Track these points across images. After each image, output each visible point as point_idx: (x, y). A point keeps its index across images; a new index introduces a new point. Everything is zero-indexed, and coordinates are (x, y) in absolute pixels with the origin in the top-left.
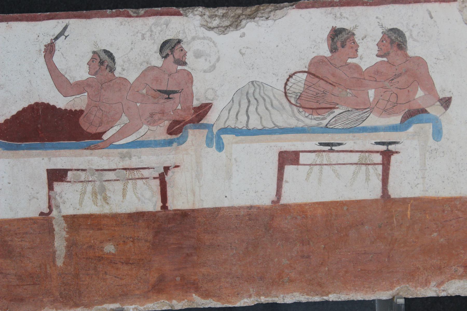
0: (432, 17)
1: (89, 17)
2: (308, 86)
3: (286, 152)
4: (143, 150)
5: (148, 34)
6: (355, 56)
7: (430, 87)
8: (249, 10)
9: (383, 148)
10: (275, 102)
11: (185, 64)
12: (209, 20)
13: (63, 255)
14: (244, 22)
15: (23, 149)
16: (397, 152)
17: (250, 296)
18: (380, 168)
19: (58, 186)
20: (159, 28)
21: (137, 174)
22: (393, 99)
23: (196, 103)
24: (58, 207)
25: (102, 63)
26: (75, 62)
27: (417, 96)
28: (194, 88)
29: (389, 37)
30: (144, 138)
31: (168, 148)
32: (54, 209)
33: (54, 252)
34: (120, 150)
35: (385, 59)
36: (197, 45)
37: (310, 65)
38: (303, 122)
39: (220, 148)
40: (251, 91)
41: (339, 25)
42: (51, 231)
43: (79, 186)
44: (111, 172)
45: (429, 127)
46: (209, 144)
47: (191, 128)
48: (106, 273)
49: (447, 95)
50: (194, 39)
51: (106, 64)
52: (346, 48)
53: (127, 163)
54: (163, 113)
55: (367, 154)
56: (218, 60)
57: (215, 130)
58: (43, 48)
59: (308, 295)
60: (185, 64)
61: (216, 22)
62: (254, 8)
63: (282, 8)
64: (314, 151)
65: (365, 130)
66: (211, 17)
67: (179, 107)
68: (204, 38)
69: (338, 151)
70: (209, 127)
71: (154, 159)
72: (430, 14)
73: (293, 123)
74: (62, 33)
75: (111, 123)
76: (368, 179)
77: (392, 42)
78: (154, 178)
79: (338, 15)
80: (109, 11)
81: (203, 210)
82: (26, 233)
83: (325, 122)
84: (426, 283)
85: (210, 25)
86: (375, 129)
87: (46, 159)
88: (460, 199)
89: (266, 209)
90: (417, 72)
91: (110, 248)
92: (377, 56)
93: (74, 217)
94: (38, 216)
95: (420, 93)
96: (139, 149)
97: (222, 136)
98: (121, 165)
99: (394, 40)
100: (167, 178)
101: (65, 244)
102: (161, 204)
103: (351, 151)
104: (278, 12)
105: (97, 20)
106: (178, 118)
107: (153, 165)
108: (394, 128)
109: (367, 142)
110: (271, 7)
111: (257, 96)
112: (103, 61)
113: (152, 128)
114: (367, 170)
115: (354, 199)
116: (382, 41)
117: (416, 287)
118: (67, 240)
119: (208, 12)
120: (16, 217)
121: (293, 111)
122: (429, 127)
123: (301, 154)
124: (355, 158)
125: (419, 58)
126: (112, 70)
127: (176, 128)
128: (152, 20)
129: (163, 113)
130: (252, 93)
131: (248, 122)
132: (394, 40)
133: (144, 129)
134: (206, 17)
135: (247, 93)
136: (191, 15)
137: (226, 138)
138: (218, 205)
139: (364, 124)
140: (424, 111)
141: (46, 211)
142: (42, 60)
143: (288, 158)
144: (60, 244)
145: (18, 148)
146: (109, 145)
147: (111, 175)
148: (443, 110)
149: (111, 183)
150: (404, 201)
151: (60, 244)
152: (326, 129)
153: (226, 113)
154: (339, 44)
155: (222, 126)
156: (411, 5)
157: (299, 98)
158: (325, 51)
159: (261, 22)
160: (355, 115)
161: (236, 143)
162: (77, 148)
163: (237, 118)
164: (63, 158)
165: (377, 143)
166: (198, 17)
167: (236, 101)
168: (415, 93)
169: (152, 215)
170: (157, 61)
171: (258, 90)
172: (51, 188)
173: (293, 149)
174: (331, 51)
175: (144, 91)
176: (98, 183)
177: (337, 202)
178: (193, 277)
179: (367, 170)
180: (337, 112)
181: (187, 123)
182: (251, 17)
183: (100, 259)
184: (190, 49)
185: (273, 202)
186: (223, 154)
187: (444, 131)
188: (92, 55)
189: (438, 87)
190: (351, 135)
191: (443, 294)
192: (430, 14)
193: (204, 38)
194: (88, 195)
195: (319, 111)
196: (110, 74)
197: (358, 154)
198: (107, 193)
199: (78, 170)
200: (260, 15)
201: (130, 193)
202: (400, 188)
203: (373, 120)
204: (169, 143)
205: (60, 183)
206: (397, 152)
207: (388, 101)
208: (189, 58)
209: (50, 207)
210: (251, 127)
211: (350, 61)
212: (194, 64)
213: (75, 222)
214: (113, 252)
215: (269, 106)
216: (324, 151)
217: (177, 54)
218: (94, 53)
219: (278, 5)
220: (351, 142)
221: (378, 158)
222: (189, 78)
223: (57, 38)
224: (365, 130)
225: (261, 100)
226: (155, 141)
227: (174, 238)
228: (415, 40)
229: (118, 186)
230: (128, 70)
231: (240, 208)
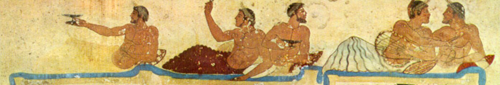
6: (427, 22)
7: (480, 49)
10: (367, 52)
11: (305, 22)
22: (452, 56)
40: (351, 44)
46: (319, 79)
49: (492, 54)
57: (324, 71)
58: (204, 5)
60: (305, 22)
75: (252, 61)
83: (402, 69)
90: (471, 36)
97: (329, 76)
99: (455, 12)
111: (355, 48)
112: (246, 15)
130: (351, 44)
132: (455, 12)
139: (432, 71)
142: (203, 14)
146: (248, 78)
148: (487, 64)
152: (403, 74)
153: (332, 58)
155: (329, 69)
157: (385, 50)
158: (405, 17)
167: (340, 51)
170: (285, 18)
180: (412, 62)
189: (485, 47)
210: (349, 70)
211: (423, 25)
212: (310, 23)
230: (264, 23)
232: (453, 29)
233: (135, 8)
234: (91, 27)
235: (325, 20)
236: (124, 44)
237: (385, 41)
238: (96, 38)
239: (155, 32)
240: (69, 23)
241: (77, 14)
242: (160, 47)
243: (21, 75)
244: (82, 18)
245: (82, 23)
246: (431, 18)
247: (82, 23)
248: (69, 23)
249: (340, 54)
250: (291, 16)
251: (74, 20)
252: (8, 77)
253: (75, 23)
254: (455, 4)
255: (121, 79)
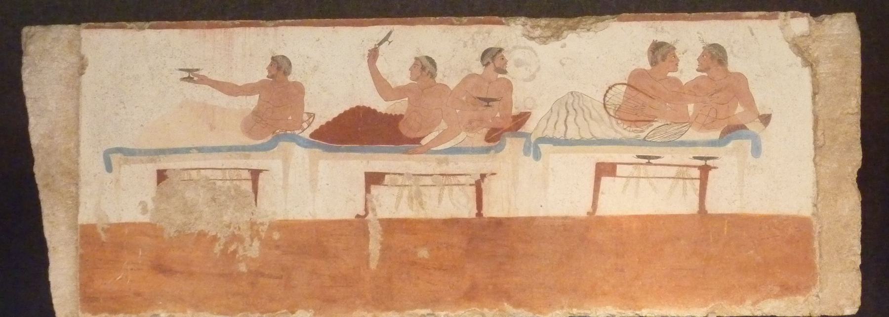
0: (753, 34)
1: (412, 24)
2: (627, 98)
3: (603, 164)
4: (461, 156)
5: (470, 42)
6: (675, 70)
7: (750, 103)
8: (571, 22)
9: (702, 163)
10: (594, 113)
12: (531, 30)
13: (377, 258)
14: (565, 33)
15: (343, 151)
16: (715, 168)
17: (562, 308)
18: (697, 183)
19: (375, 190)
20: (481, 36)
21: (453, 180)
22: (713, 114)
23: (515, 112)
24: (374, 210)
25: (423, 68)
26: (397, 67)
27: (737, 112)
28: (513, 96)
29: (709, 52)
30: (462, 145)
31: (486, 155)
32: (370, 212)
33: (369, 255)
34: (438, 156)
35: (705, 74)
36: (518, 55)
37: (630, 77)
38: (620, 133)
39: (537, 156)
41: (660, 38)
42: (366, 234)
43: (396, 190)
44: (427, 178)
45: (748, 144)
46: (526, 153)
47: (509, 136)
48: (418, 278)
50: (515, 48)
51: (427, 70)
52: (667, 61)
53: (444, 169)
54: (481, 120)
55: (685, 168)
56: (539, 69)
57: (533, 139)
58: (367, 53)
59: (620, 308)
60: (505, 72)
61: (538, 32)
62: (576, 20)
63: (604, 20)
64: (631, 164)
65: (683, 144)
66: (533, 27)
67: (498, 115)
68: (525, 48)
69: (655, 165)
70: (527, 136)
71: (472, 165)
72: (751, 31)
73: (611, 135)
74: (385, 39)
76: (685, 194)
77: (712, 57)
78: (471, 185)
79: (660, 29)
80: (432, 19)
81: (517, 218)
82: (342, 235)
83: (643, 135)
84: (742, 301)
85: (532, 35)
86: (694, 144)
87: (365, 162)
88: (777, 217)
89: (581, 220)
90: (736, 89)
91: (423, 253)
92: (698, 70)
93: (389, 221)
94: (353, 217)
95: (740, 109)
96: (456, 156)
98: (439, 170)
99: (715, 56)
100: (483, 186)
101: (379, 248)
102: (476, 211)
103: (669, 165)
104: (600, 24)
105: (420, 26)
106: (497, 126)
107: (469, 172)
108: (712, 143)
109: (685, 156)
110: (593, 19)
111: (576, 107)
112: (425, 67)
113: (471, 135)
114: (685, 187)
115: (670, 213)
116: (703, 55)
117: (730, 305)
118: (381, 244)
119: (530, 22)
120: (333, 218)
121: (611, 124)
122: (748, 144)
123: (618, 166)
124: (673, 171)
125: (740, 74)
126: (433, 76)
127: (495, 136)
128: (474, 28)
129: (481, 120)
130: (571, 104)
131: (566, 132)
132: (715, 56)
133: (462, 136)
134: (528, 27)
135: (566, 103)
136: (513, 25)
137: (543, 147)
138: (533, 214)
139: (683, 138)
140: (743, 127)
141: (362, 213)
143: (604, 170)
144: (374, 247)
145: (338, 150)
146: (427, 150)
147: (428, 181)
149: (426, 188)
150: (721, 217)
151: (374, 247)
152: (644, 142)
153: (543, 124)
154: (659, 57)
155: (540, 135)
156: (732, 22)
157: (618, 109)
158: (645, 64)
159: (582, 34)
160: (674, 129)
161: (554, 152)
162: (396, 152)
163: (555, 128)
164: (380, 162)
165: (695, 158)
166: (520, 27)
168: (735, 108)
169: (467, 222)
171: (577, 101)
172: (368, 190)
173: (611, 160)
174: (651, 64)
175: (464, 98)
176: (414, 188)
177: (653, 216)
178: (506, 286)
179: (685, 187)
180: (656, 125)
181: (506, 131)
182: (573, 28)
183: (414, 263)
184: (511, 58)
185: (588, 213)
186: (540, 163)
187: (764, 147)
188: (413, 60)
189: (758, 104)
190: (669, 149)
191: (759, 313)
192: (751, 31)
193: (525, 48)
194: (405, 199)
195: (638, 124)
196: (431, 80)
197: (676, 168)
198: (423, 198)
199: (395, 174)
200: (582, 26)
201: (446, 199)
202: (717, 205)
203: (692, 134)
204: (487, 150)
205: (378, 186)
206: (715, 168)
207: (708, 116)
208: (510, 68)
209: (366, 210)
210: (569, 137)
211: (670, 74)
213: (390, 226)
214: (426, 257)
215: (587, 117)
216: (642, 164)
217: (498, 62)
218: (416, 59)
219: (600, 17)
220: (668, 155)
221: (696, 173)
222: (509, 87)
223: (380, 44)
224: (683, 144)
225: (579, 111)
226: (473, 148)
227: (489, 247)
228: (735, 56)
229: (435, 191)
230: (449, 76)
231: (555, 218)
232: (712, 79)
233: (273, 58)
234: (216, 85)
235: (534, 69)
236: (259, 105)
237: (619, 94)
238: (220, 99)
239: (300, 89)
240: (184, 79)
241: (196, 68)
242: (307, 109)
243: (119, 150)
244: (201, 73)
245: (203, 80)
246: (681, 65)
247: (203, 80)
248: (184, 79)
249: (555, 114)
250: (487, 65)
251: (192, 76)
252: (102, 153)
253: (189, 79)
254: (715, 46)
255: (253, 154)
